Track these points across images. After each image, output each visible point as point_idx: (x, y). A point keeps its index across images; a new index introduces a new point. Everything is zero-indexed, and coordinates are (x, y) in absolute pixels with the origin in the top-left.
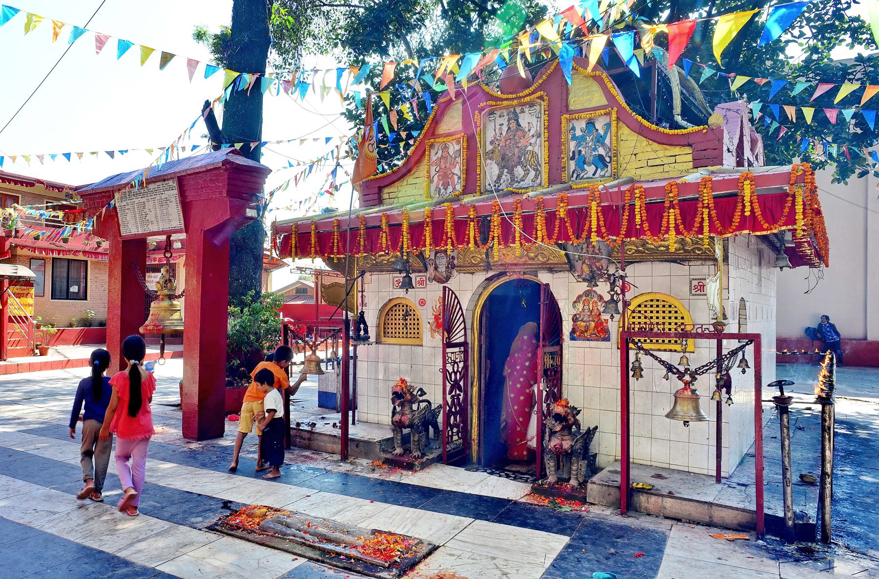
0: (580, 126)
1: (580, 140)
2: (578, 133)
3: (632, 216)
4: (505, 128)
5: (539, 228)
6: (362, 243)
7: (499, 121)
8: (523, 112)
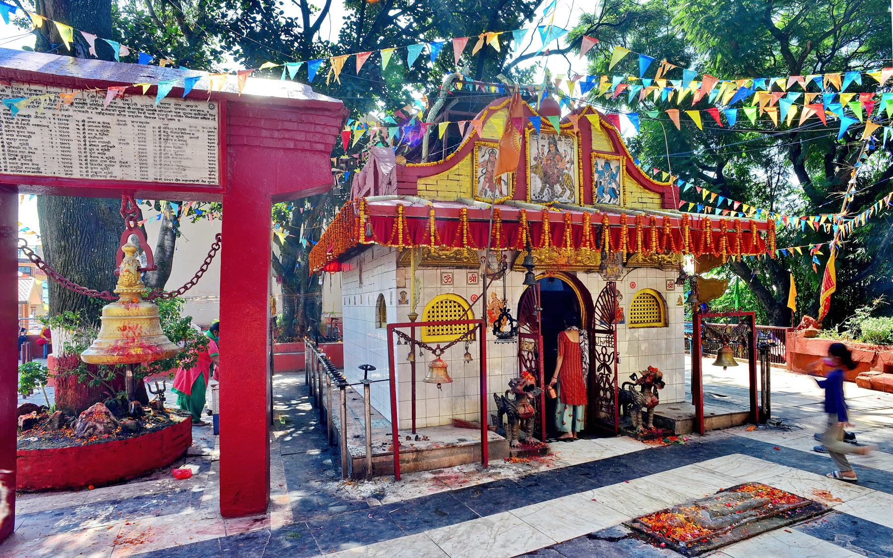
0: (601, 163)
1: (601, 174)
2: (600, 169)
3: (706, 238)
4: (546, 150)
5: (654, 239)
6: (498, 237)
7: (542, 142)
8: (560, 140)
